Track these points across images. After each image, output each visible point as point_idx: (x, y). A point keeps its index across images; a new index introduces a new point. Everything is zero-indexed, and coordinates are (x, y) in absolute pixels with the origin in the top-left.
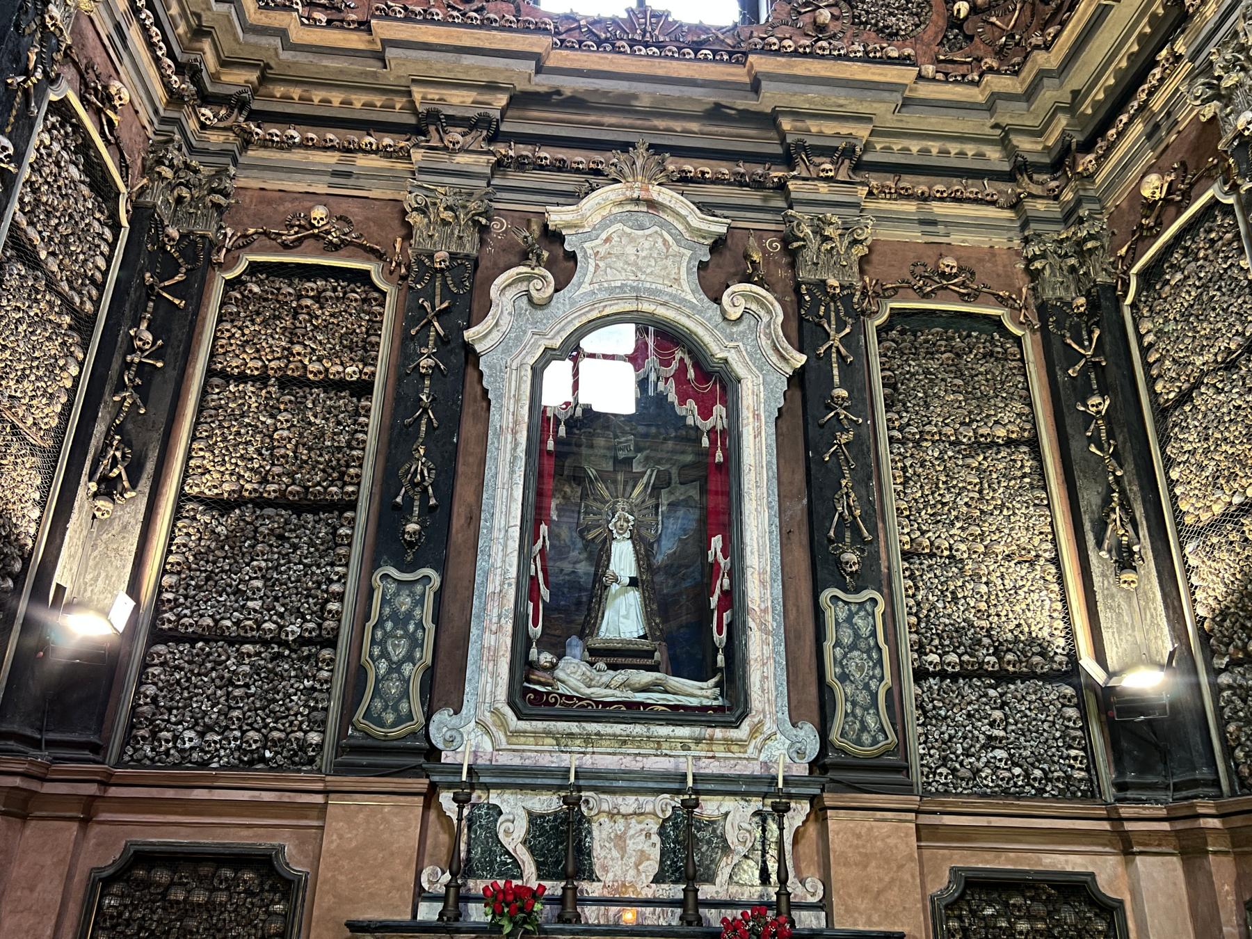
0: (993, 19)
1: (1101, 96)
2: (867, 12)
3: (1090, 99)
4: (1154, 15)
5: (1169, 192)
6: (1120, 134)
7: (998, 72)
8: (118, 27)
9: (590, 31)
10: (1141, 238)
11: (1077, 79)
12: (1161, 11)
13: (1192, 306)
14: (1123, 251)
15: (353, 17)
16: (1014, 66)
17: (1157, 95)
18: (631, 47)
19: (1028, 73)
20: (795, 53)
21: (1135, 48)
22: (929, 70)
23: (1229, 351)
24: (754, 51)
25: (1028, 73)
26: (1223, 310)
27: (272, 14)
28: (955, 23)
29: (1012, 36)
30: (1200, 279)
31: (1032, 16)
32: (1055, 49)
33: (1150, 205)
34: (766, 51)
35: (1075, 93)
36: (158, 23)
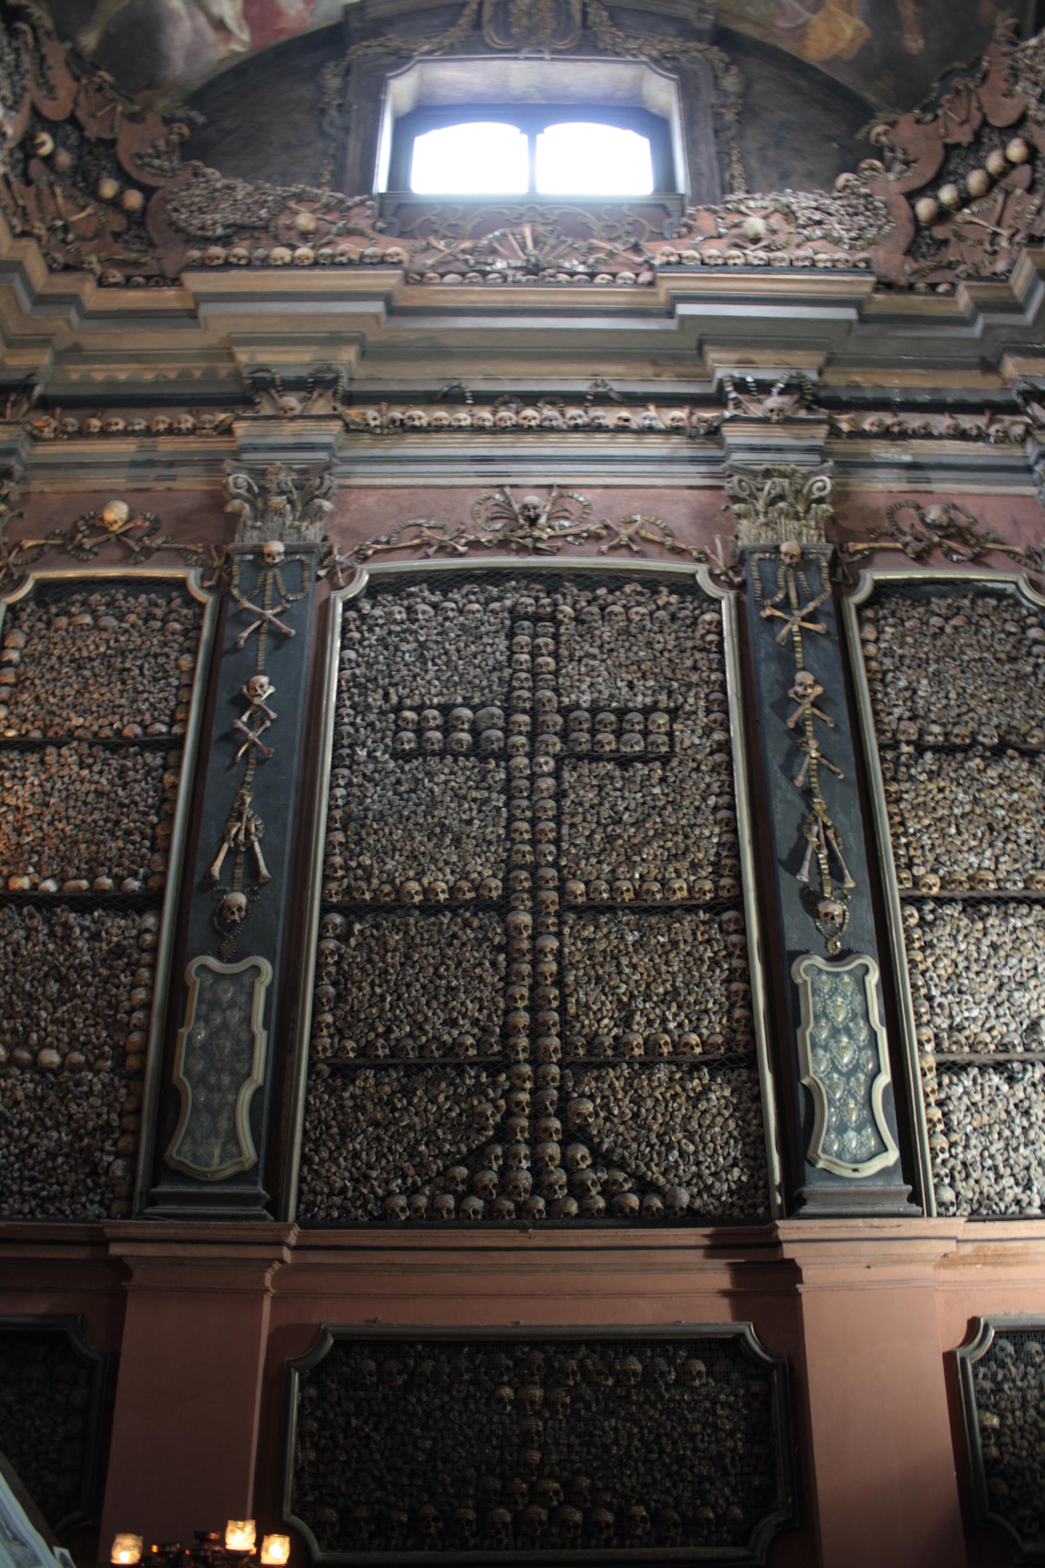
5: (125, 534)
6: (105, 433)
10: (62, 549)
11: (97, 339)
13: (91, 659)
14: (29, 543)
17: (169, 438)
19: (64, 283)
23: (119, 732)
26: (135, 689)
29: (66, 229)
30: (117, 641)
33: (99, 527)
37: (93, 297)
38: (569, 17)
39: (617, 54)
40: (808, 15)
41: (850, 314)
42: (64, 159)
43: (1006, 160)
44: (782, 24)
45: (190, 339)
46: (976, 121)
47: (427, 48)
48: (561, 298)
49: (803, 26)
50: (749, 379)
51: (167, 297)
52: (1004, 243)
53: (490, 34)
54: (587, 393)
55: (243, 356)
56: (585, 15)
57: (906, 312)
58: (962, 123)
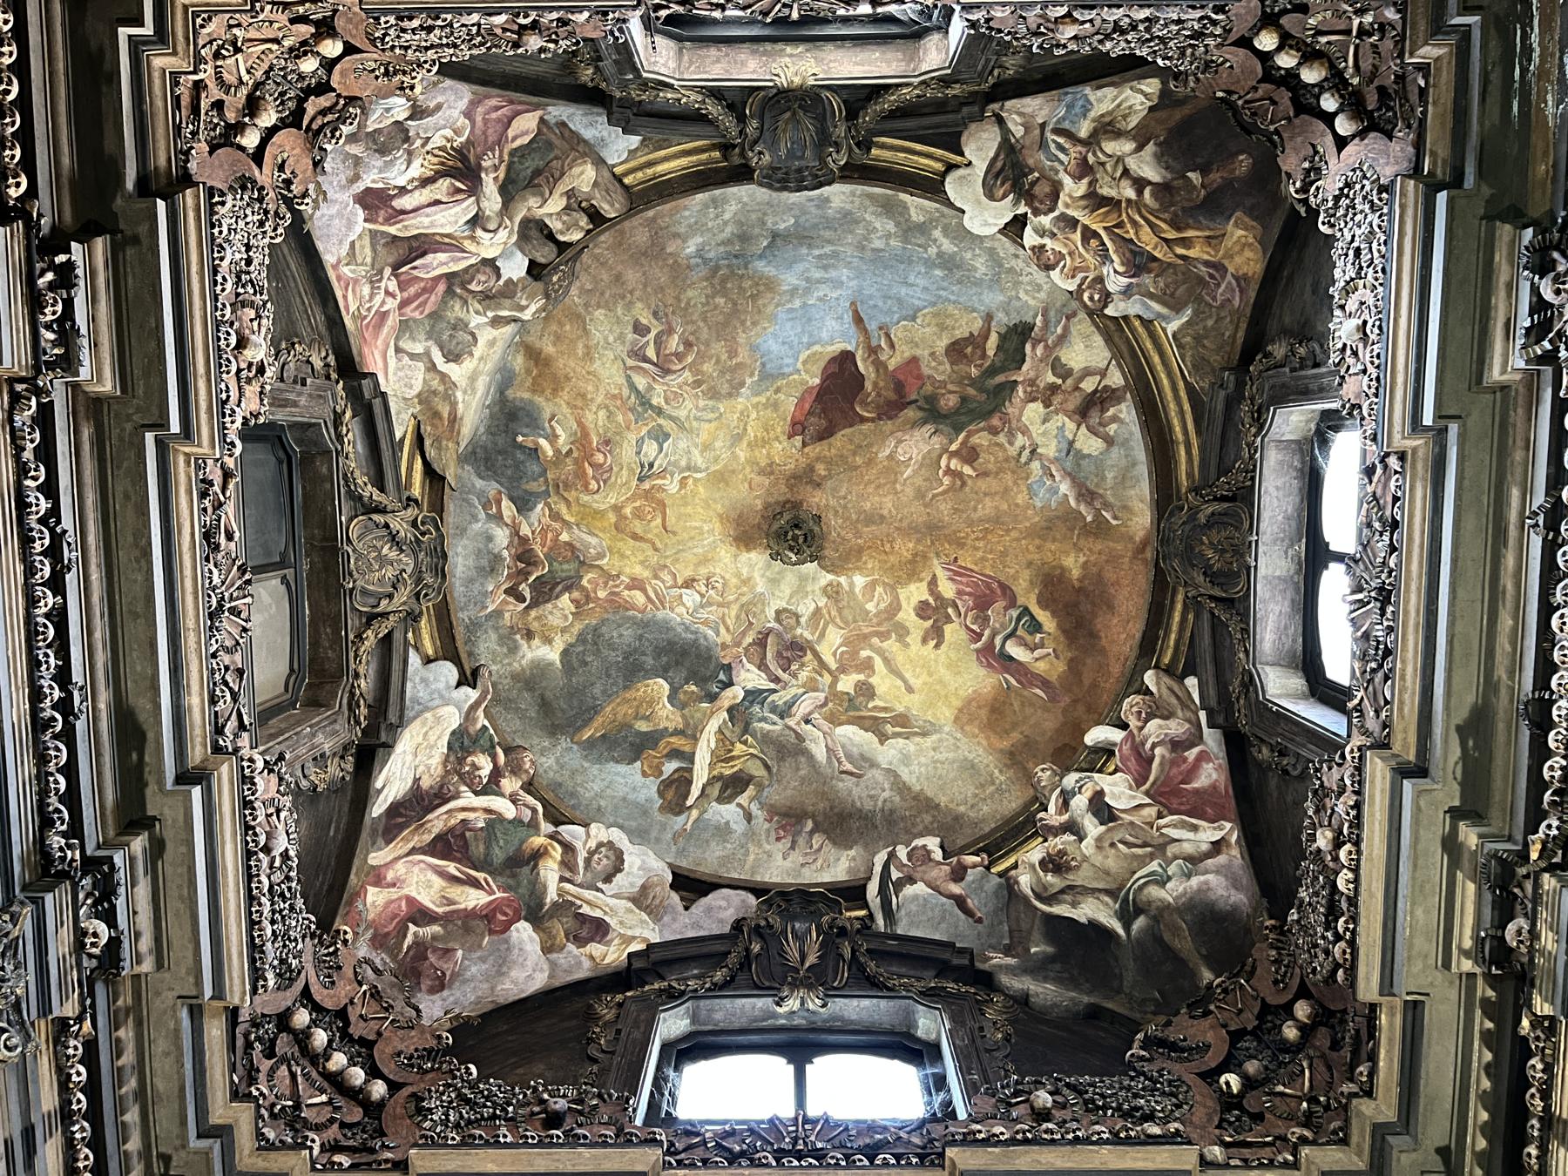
0: (1280, 1088)
1: (1482, 1144)
2: (1103, 1096)
3: (1468, 1153)
4: (1485, 1002)
7: (1314, 1143)
8: (28, 1133)
9: (718, 1145)
11: (1436, 1129)
12: (1490, 993)
15: (390, 1155)
16: (1335, 1132)
18: (778, 1160)
19: (1360, 1135)
20: (1012, 1142)
21: (1488, 1056)
22: (1216, 1152)
24: (953, 1143)
25: (1360, 1135)
27: (273, 1155)
28: (1229, 1102)
31: (1329, 1068)
32: (1380, 1091)
34: (969, 1140)
35: (1443, 1152)
36: (97, 1143)
37: (1382, 1107)
38: (1225, 514)
39: (1254, 470)
40: (1229, 277)
41: (1442, 198)
42: (1252, 1067)
43: (1279, 49)
44: (1236, 302)
45: (1443, 1014)
46: (1265, 88)
47: (1242, 655)
48: (1416, 567)
49: (1237, 278)
50: (1527, 323)
51: (1389, 1024)
52: (1368, 18)
53: (1236, 591)
54: (1545, 540)
55: (1467, 965)
56: (1223, 499)
57: (1450, 125)
58: (1274, 103)
